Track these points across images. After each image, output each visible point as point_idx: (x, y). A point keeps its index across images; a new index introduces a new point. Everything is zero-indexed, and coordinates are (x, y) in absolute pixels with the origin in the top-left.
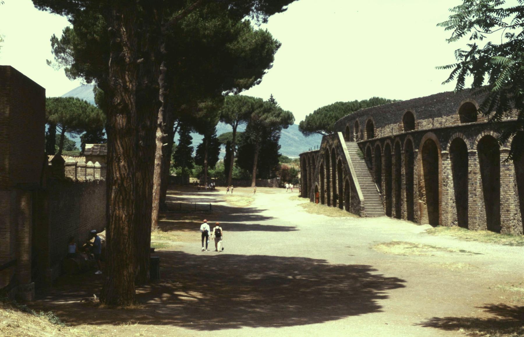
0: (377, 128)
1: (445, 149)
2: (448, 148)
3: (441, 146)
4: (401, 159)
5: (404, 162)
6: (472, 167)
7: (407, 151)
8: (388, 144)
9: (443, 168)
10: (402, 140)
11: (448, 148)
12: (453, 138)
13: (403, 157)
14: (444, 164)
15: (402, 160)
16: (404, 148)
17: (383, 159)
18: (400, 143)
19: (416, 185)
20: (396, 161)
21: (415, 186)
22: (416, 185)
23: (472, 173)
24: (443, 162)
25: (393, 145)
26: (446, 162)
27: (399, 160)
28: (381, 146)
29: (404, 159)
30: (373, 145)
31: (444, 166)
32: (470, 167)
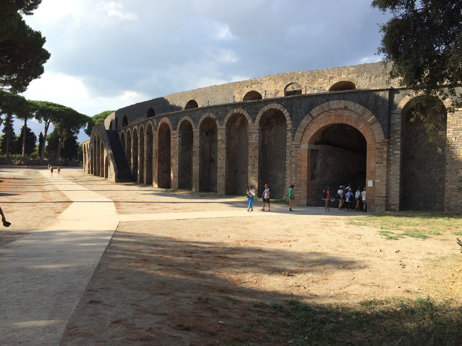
0: (130, 121)
1: (176, 130)
2: (178, 129)
3: (173, 128)
4: (144, 139)
5: (146, 141)
6: (196, 142)
7: (148, 134)
8: (135, 129)
9: (175, 144)
10: (145, 125)
11: (178, 129)
12: (181, 120)
13: (145, 138)
14: (174, 141)
15: (145, 140)
16: (146, 131)
17: (132, 140)
18: (144, 128)
19: (154, 158)
20: (141, 141)
21: (153, 159)
22: (154, 158)
23: (196, 147)
24: (174, 140)
25: (138, 130)
26: (176, 139)
27: (142, 140)
28: (130, 132)
29: (146, 139)
30: (125, 131)
31: (175, 142)
32: (195, 143)
